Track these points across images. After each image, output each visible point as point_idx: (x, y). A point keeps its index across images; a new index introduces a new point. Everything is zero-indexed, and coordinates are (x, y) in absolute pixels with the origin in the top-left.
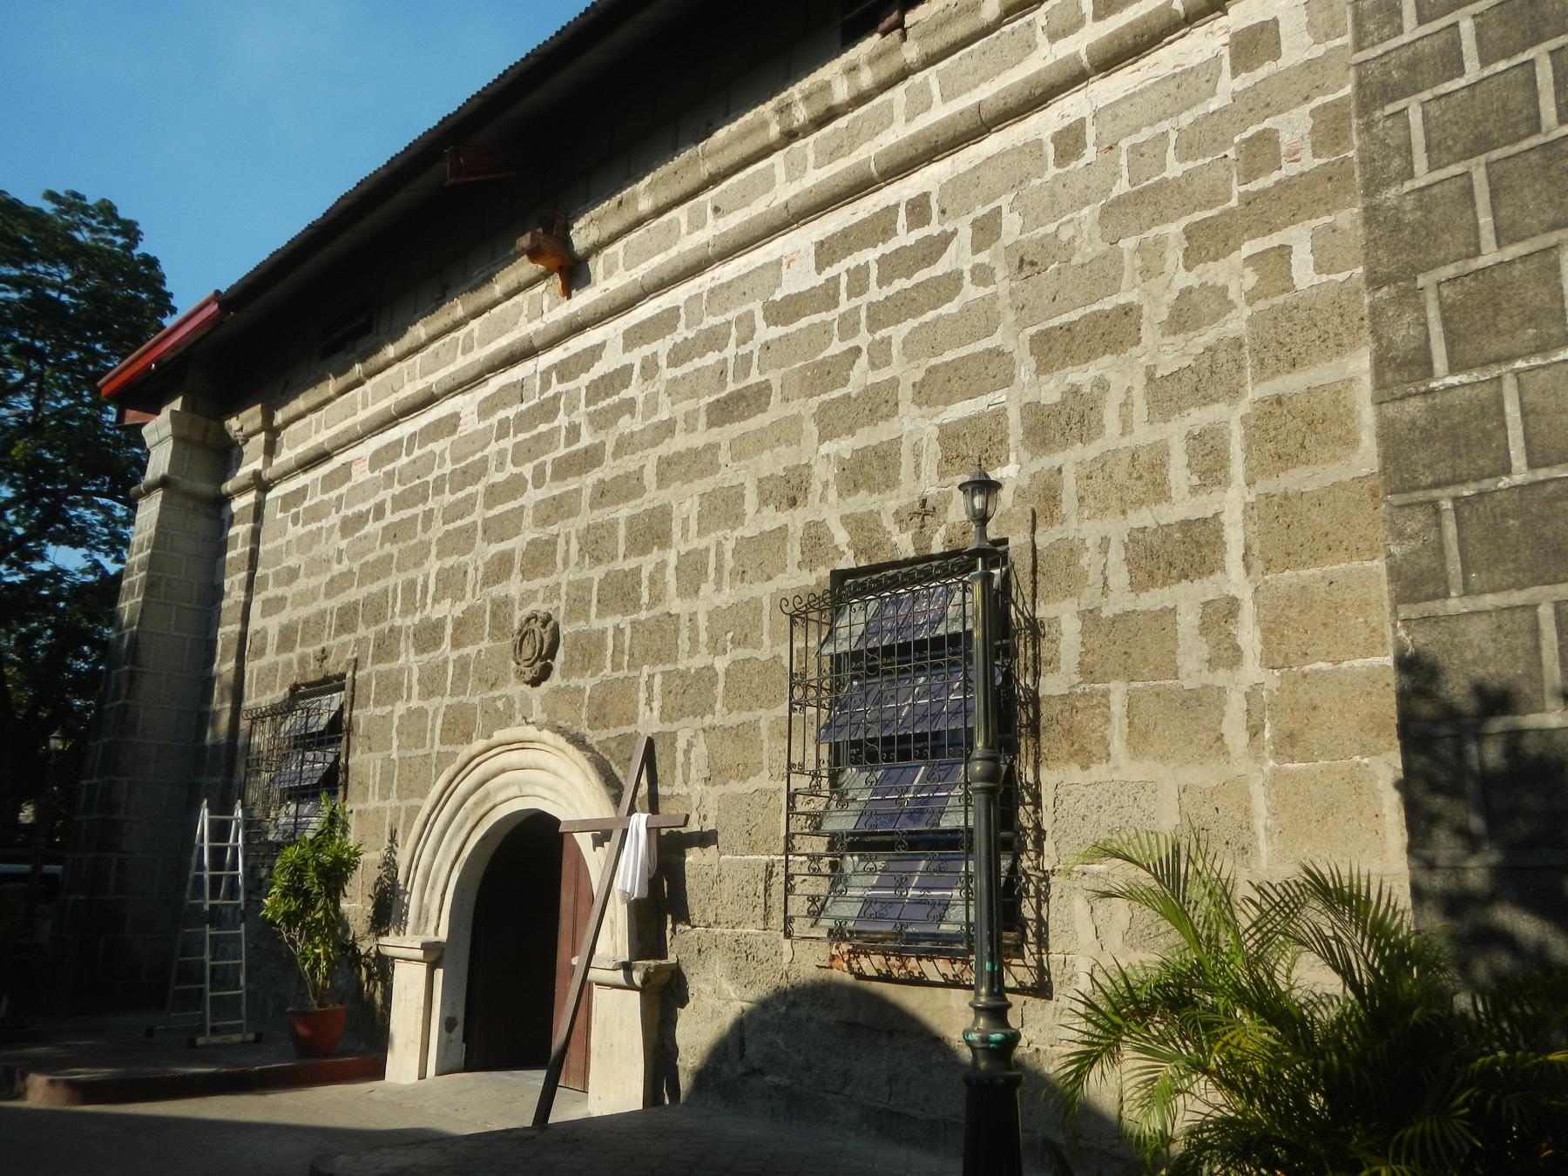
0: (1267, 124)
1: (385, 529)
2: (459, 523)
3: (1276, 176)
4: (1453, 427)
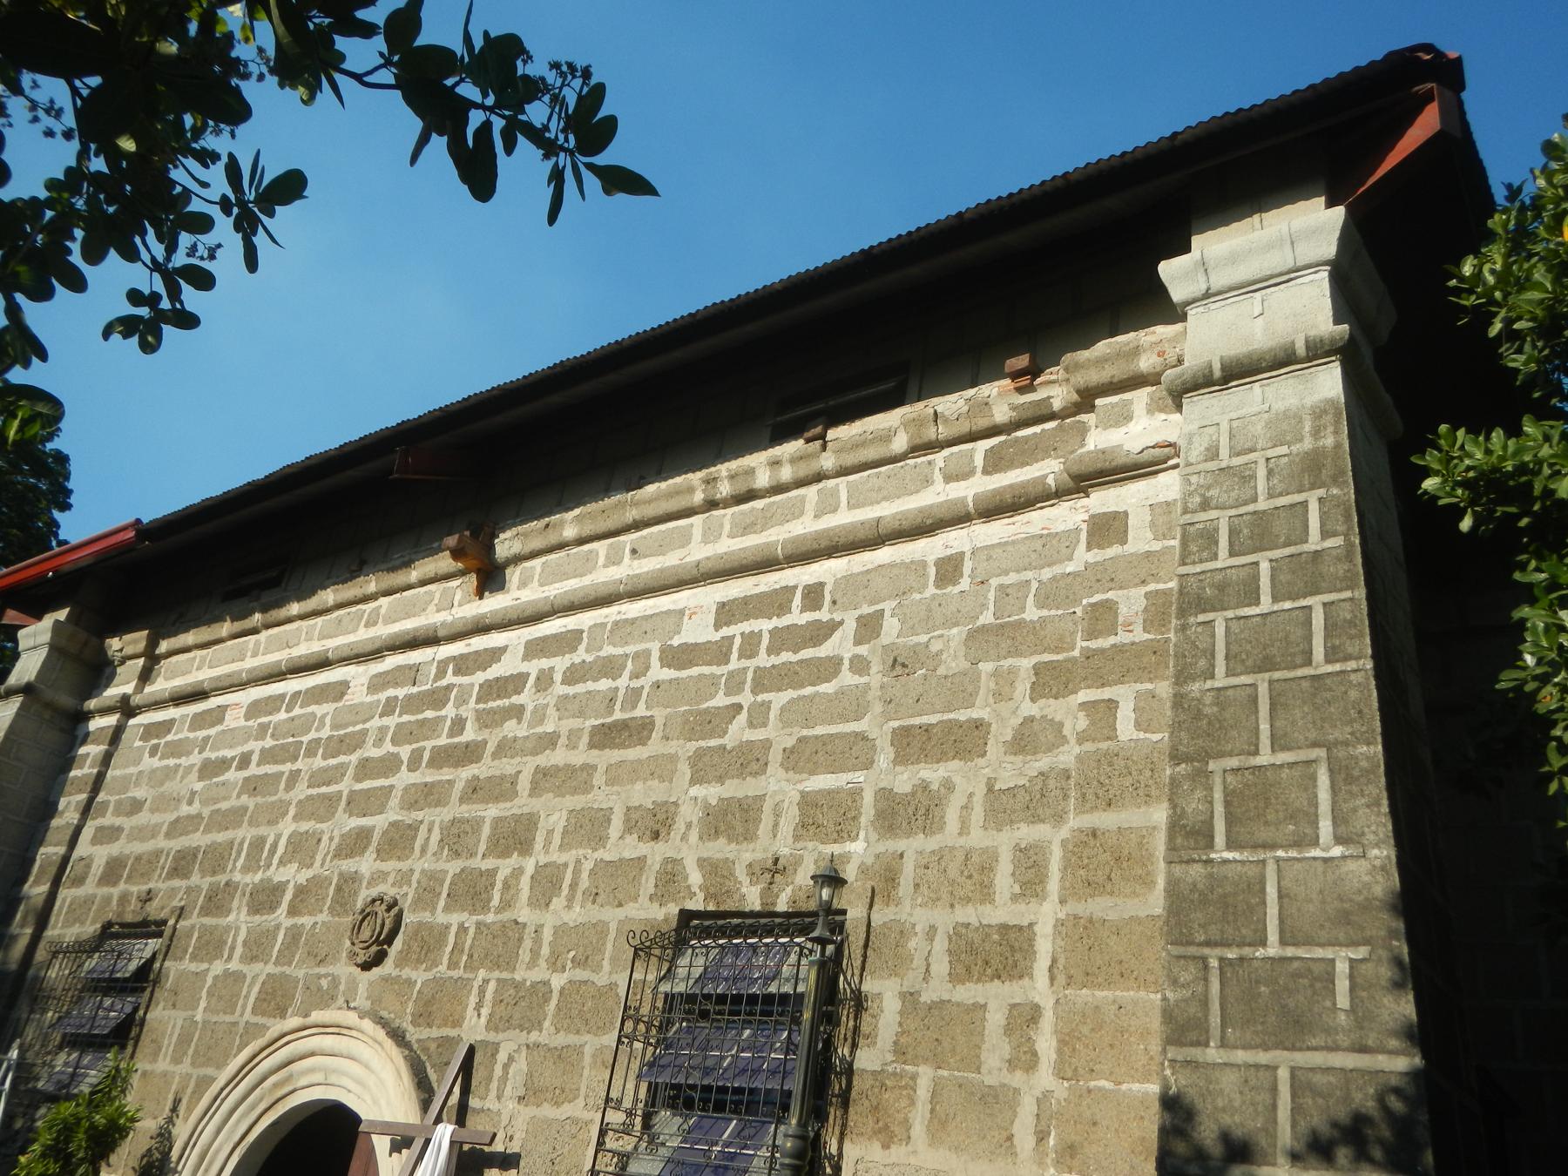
0: (1110, 595)
1: (246, 779)
2: (324, 790)
3: (1112, 640)
4: (1225, 896)
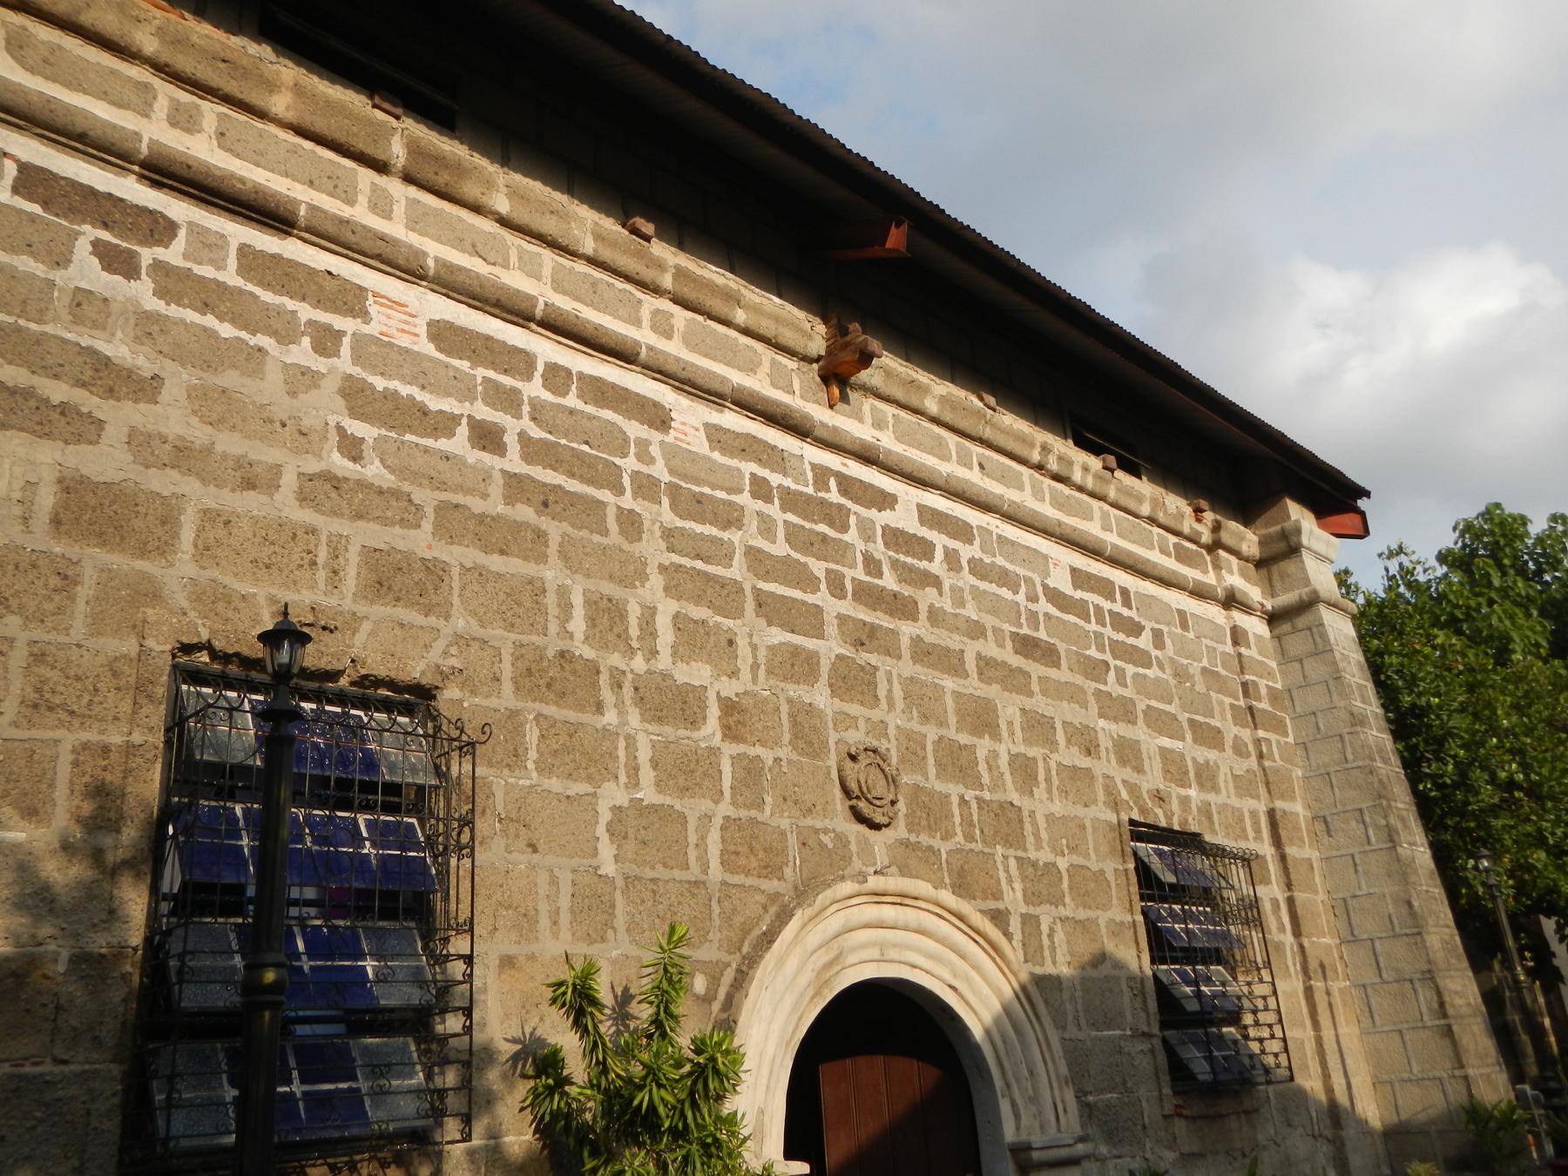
2: (699, 565)
